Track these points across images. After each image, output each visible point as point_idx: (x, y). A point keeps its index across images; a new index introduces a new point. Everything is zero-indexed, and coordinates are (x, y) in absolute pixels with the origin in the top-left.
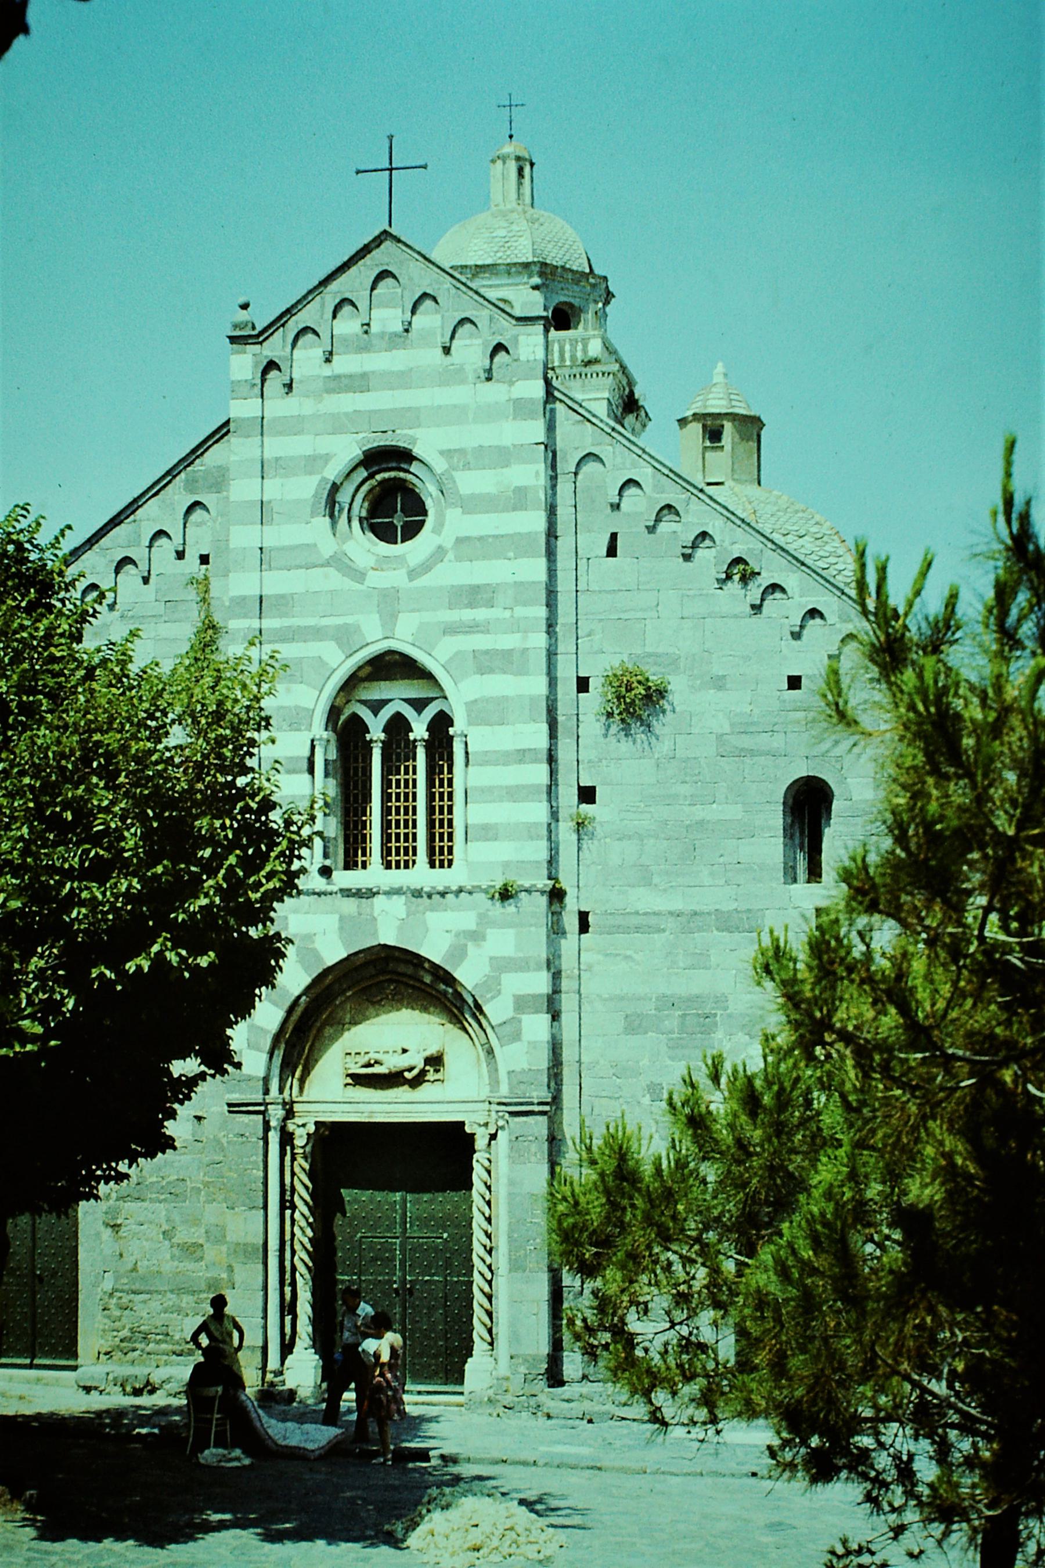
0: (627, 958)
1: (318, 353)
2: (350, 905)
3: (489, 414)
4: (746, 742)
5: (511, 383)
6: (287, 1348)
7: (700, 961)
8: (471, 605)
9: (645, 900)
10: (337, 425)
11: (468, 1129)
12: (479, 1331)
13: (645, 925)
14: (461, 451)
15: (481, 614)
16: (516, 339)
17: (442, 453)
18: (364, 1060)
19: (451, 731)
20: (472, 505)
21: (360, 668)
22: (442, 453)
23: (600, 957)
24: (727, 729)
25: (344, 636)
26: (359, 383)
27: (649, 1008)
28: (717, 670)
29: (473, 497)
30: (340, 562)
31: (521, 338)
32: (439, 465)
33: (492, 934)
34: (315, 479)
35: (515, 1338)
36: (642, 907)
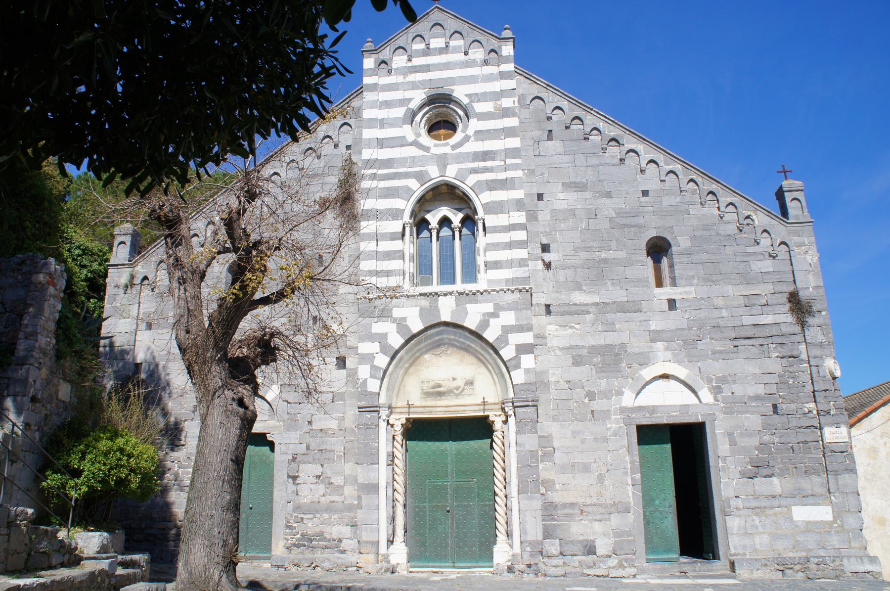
0: (572, 327)
1: (406, 57)
2: (425, 302)
3: (489, 78)
4: (624, 221)
5: (499, 66)
6: (391, 542)
7: (610, 327)
8: (484, 160)
9: (579, 298)
10: (414, 86)
11: (491, 419)
12: (501, 528)
13: (579, 310)
14: (476, 94)
15: (489, 164)
16: (500, 47)
17: (466, 95)
18: (432, 384)
19: (476, 217)
20: (483, 116)
21: (427, 192)
22: (466, 95)
23: (557, 327)
24: (614, 215)
25: (420, 177)
26: (426, 68)
27: (585, 352)
28: (607, 189)
29: (482, 113)
30: (415, 144)
31: (503, 47)
32: (465, 101)
33: (501, 314)
34: (405, 108)
35: (523, 531)
36: (578, 302)
